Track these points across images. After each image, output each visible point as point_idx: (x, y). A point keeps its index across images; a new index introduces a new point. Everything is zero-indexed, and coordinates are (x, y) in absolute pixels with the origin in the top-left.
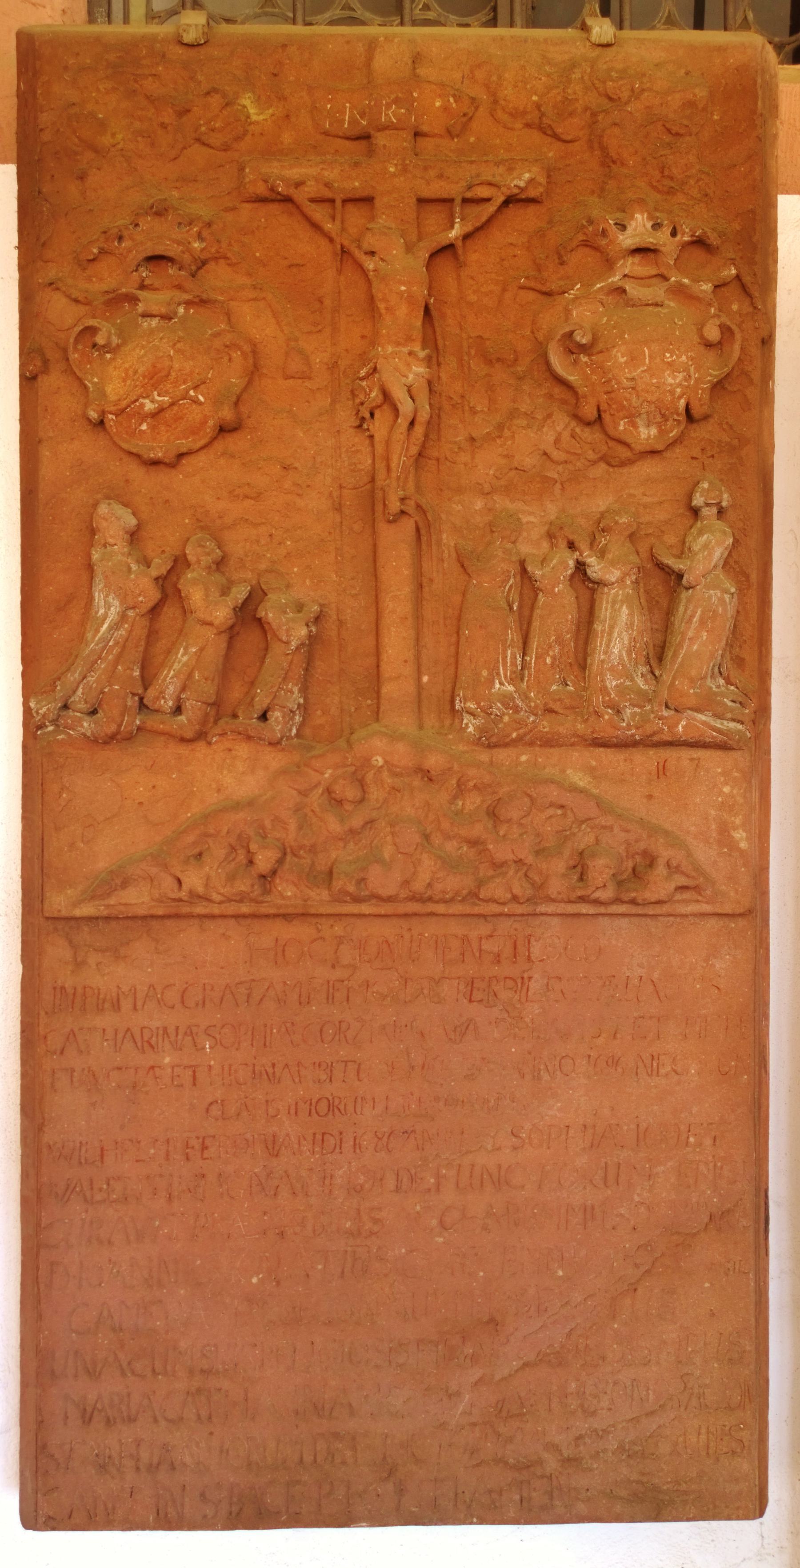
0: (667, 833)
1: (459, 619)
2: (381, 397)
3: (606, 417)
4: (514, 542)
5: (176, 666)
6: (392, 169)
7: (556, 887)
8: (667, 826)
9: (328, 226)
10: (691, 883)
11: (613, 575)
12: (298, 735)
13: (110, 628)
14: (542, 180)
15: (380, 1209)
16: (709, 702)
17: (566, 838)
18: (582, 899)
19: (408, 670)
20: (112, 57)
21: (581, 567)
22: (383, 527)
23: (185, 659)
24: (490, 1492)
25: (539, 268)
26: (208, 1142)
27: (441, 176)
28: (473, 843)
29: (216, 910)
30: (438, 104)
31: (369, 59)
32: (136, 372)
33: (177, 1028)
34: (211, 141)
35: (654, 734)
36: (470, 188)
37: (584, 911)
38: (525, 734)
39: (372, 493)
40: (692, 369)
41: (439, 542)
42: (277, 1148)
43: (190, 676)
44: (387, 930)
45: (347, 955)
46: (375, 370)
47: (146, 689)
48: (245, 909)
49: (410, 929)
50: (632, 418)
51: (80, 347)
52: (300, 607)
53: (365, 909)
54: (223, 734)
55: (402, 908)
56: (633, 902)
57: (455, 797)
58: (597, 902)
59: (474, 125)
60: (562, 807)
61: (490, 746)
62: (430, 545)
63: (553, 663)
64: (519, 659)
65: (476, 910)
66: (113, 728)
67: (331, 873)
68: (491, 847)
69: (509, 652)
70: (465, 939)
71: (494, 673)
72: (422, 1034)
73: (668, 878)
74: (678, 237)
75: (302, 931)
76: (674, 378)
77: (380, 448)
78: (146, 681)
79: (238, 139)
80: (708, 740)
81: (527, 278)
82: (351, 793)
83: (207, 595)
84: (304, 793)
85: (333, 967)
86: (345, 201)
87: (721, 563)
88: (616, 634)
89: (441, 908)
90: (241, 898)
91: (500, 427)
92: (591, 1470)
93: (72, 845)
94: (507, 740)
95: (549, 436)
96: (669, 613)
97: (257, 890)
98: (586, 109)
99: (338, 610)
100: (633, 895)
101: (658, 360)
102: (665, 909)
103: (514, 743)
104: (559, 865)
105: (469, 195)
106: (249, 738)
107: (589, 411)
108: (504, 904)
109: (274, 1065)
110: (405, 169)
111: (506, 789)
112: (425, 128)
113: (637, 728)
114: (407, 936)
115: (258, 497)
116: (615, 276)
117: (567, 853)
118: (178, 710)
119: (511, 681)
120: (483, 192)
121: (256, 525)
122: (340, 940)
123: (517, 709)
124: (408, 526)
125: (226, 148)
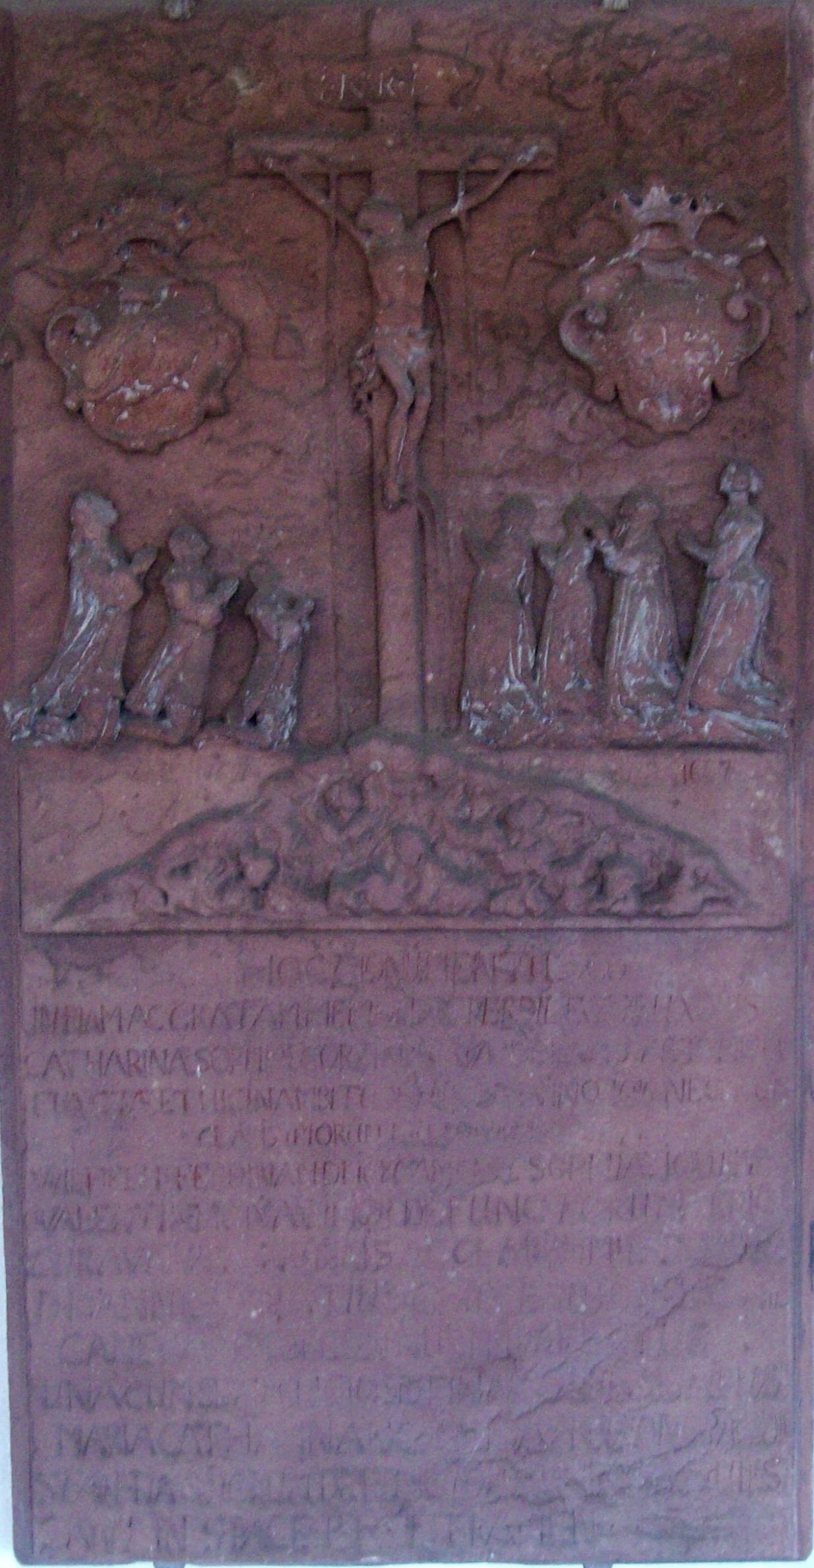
0: (693, 841)
1: (466, 613)
2: (378, 379)
3: (625, 398)
5: (159, 667)
7: (573, 901)
9: (321, 202)
10: (721, 895)
11: (633, 566)
14: (553, 150)
16: (737, 700)
18: (604, 913)
19: (412, 666)
20: (95, 34)
21: (598, 557)
23: (169, 659)
27: (443, 149)
28: (483, 853)
29: (206, 925)
30: (440, 73)
31: (366, 34)
32: (116, 360)
33: (165, 1052)
35: (678, 735)
36: (473, 160)
37: (605, 926)
38: (538, 736)
40: (716, 348)
44: (389, 947)
46: (372, 351)
47: (127, 690)
48: (235, 924)
49: (416, 946)
50: (653, 397)
51: (58, 333)
52: (292, 603)
53: (367, 924)
54: (210, 739)
56: (658, 915)
58: (619, 916)
60: (579, 814)
61: (500, 749)
63: (567, 662)
64: (531, 657)
65: (488, 925)
66: (93, 734)
67: (327, 885)
68: (501, 857)
69: (520, 649)
71: (502, 673)
74: (699, 210)
75: (297, 948)
76: (696, 357)
78: (128, 684)
80: (736, 741)
81: (539, 249)
82: (349, 800)
83: (192, 590)
85: (333, 987)
86: (339, 177)
87: (751, 551)
88: (634, 629)
89: (448, 923)
90: (231, 914)
93: (52, 859)
96: (697, 603)
97: (248, 906)
98: (597, 78)
100: (657, 907)
101: (677, 340)
103: (524, 745)
104: (577, 876)
105: (472, 168)
107: (604, 390)
108: (518, 918)
110: (402, 144)
111: (516, 796)
116: (630, 249)
117: (586, 861)
118: (162, 714)
119: (522, 680)
120: (487, 164)
121: (245, 514)
123: (528, 712)
124: (409, 515)
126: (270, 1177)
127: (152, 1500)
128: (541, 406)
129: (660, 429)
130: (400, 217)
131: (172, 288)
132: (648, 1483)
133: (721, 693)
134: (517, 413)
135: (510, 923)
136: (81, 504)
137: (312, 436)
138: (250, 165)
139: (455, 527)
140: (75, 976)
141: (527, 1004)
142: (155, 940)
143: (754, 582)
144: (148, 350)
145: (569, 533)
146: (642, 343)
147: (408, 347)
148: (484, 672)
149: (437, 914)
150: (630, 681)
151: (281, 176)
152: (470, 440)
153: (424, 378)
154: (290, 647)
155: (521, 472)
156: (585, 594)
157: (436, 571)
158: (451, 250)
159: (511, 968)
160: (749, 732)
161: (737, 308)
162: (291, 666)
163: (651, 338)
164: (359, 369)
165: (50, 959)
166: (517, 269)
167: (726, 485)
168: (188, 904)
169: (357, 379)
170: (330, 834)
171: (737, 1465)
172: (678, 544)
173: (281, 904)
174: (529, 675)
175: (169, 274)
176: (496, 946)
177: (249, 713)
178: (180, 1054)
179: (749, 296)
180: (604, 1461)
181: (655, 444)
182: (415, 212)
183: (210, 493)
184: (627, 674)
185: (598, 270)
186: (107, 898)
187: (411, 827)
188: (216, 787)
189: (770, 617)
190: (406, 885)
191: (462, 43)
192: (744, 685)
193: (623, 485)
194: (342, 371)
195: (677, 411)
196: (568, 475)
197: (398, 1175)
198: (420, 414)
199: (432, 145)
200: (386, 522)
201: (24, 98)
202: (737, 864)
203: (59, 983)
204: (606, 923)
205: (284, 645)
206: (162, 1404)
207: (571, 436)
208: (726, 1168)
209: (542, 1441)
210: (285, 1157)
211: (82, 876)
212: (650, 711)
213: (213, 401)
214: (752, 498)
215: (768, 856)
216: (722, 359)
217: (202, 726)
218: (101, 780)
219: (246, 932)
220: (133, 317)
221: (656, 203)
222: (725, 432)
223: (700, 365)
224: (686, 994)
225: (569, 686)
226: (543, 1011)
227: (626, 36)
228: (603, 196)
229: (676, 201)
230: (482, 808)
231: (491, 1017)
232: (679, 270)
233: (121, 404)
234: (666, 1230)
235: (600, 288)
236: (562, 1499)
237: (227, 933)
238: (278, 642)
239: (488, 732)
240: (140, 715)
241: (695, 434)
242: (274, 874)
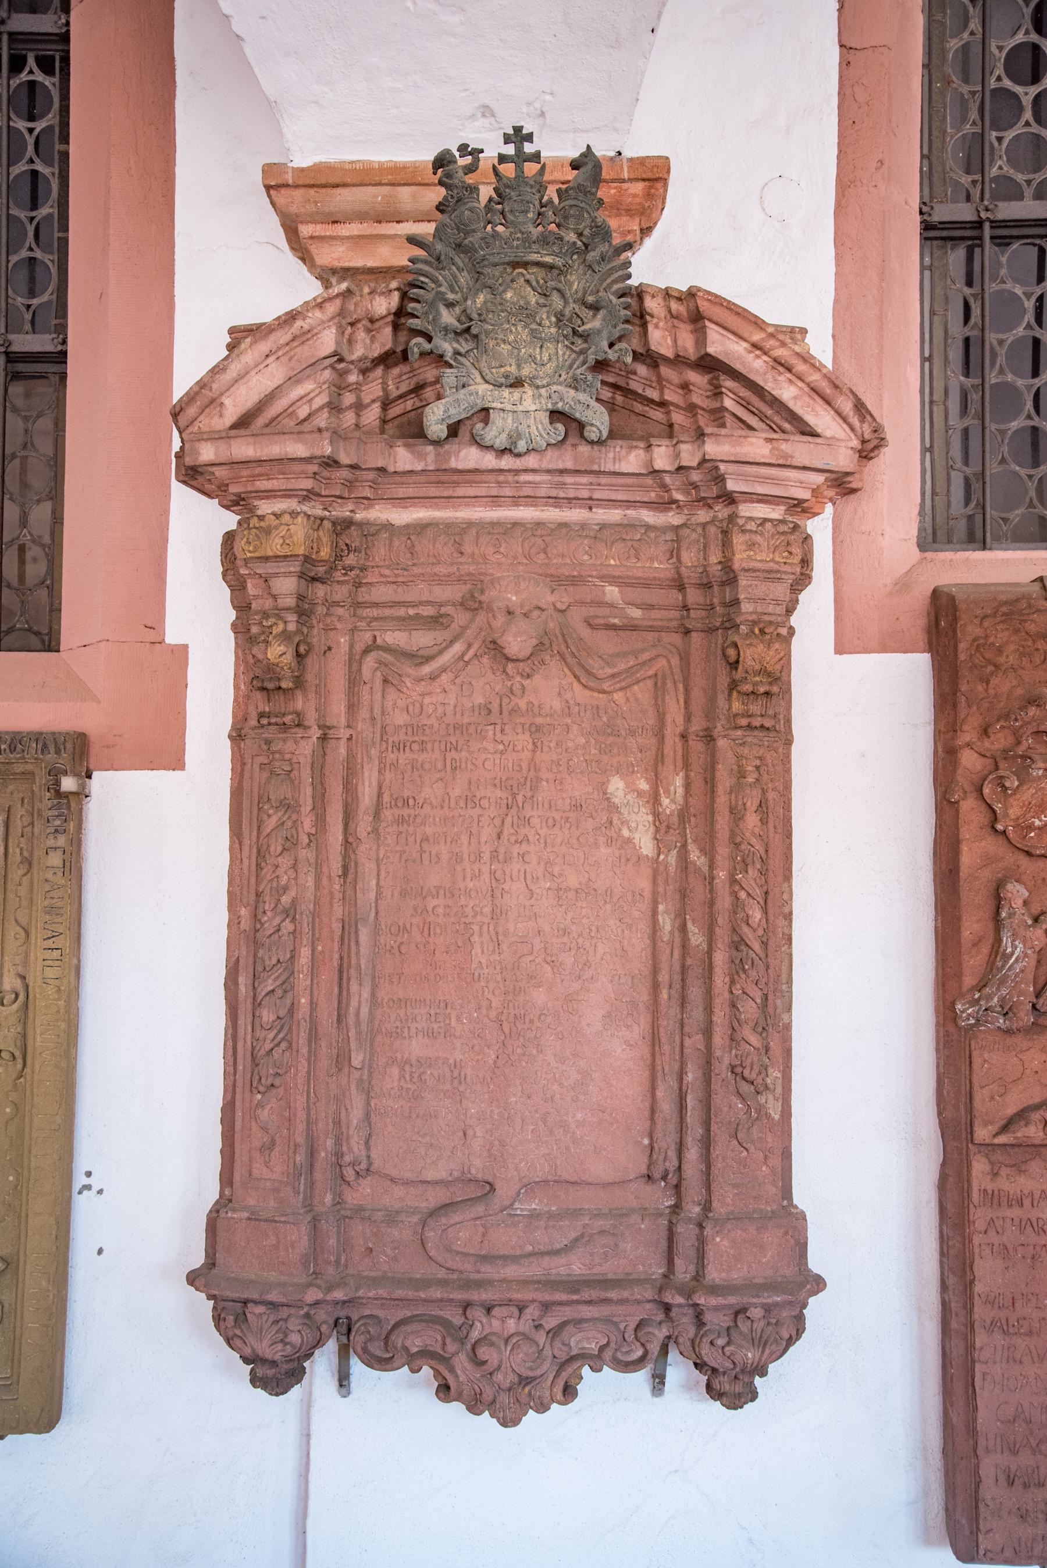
13: (1017, 960)
20: (1004, 609)
93: (992, 1098)
140: (1004, 1171)
165: (989, 1160)
201: (962, 646)
203: (995, 1175)
211: (1011, 1110)
218: (1022, 1052)
220: (1039, 778)
233: (1031, 827)
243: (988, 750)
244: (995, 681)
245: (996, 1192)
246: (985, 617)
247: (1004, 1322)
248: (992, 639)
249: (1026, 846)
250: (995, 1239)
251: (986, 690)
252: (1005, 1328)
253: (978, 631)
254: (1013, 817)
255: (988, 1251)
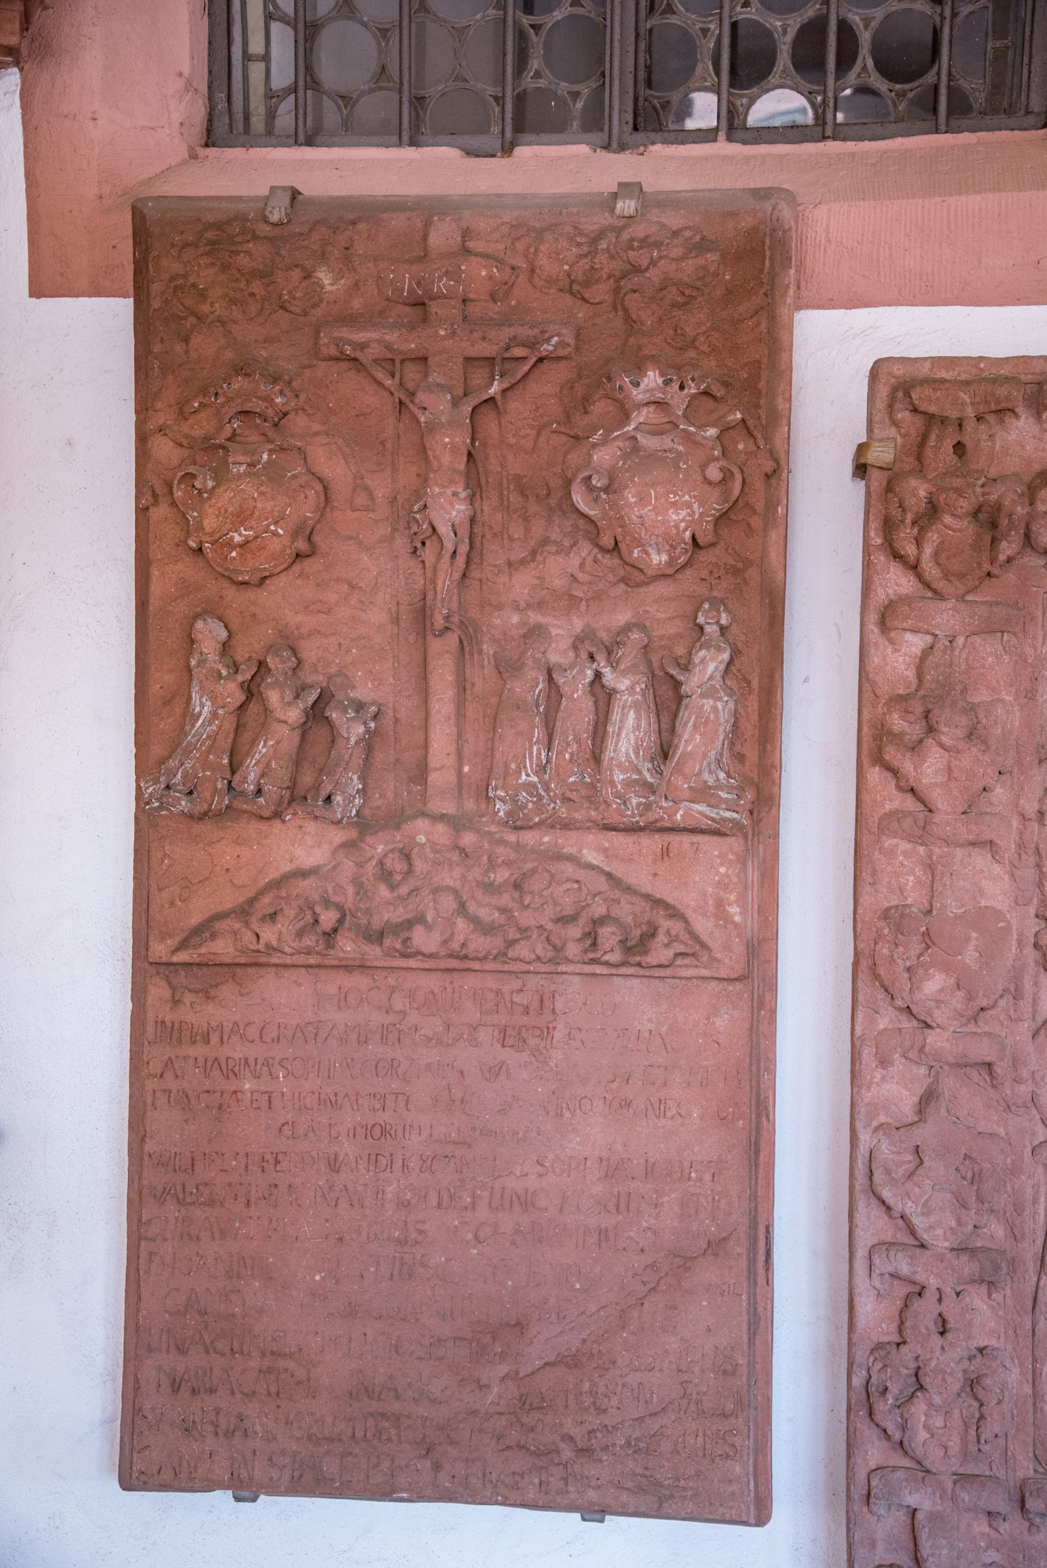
0: (667, 906)
1: (495, 718)
2: (430, 530)
3: (622, 546)
4: (544, 653)
5: (257, 756)
6: (442, 333)
7: (573, 950)
8: (669, 900)
9: (389, 382)
10: (689, 951)
11: (623, 684)
12: (358, 814)
15: (424, 1222)
16: (703, 793)
17: (583, 908)
18: (594, 961)
19: (451, 761)
20: (210, 235)
21: (598, 675)
22: (430, 638)
23: (264, 751)
24: (514, 1473)
25: (568, 416)
26: (280, 1157)
27: (484, 339)
28: (503, 910)
29: (289, 961)
30: (483, 273)
31: (425, 237)
33: (256, 1059)
34: (292, 309)
35: (656, 821)
36: (508, 348)
38: (546, 819)
39: (423, 609)
40: (696, 506)
41: (480, 652)
42: (338, 1165)
43: (268, 765)
44: (431, 982)
45: (399, 1002)
46: (425, 506)
47: (233, 773)
48: (312, 960)
49: (452, 982)
51: (183, 486)
52: (360, 707)
53: (412, 963)
54: (295, 814)
55: (444, 964)
56: (639, 965)
57: (487, 872)
58: (607, 964)
59: (516, 291)
60: (577, 882)
61: (517, 828)
62: (471, 654)
63: (571, 760)
65: (506, 968)
66: (205, 807)
68: (516, 914)
69: (535, 748)
70: (498, 992)
71: (521, 766)
72: (461, 1072)
73: (667, 946)
74: (686, 391)
75: (360, 981)
76: (678, 514)
77: (429, 574)
79: (314, 306)
80: (703, 827)
82: (398, 866)
83: (283, 698)
84: (360, 865)
85: (387, 1012)
86: (403, 361)
88: (623, 735)
89: (476, 965)
91: (534, 553)
92: (601, 1461)
93: (172, 903)
94: (531, 824)
95: (576, 561)
97: (321, 946)
98: (609, 277)
99: (395, 710)
100: (638, 959)
102: (668, 972)
103: (538, 825)
104: (575, 931)
105: (507, 355)
106: (316, 817)
107: (607, 541)
108: (529, 963)
109: (336, 1095)
110: (454, 333)
111: (529, 866)
112: (472, 296)
113: (641, 816)
114: (449, 989)
115: (329, 612)
116: (629, 425)
117: (582, 921)
118: (259, 792)
119: (536, 774)
120: (518, 352)
121: (326, 636)
122: (393, 990)
123: (540, 797)
124: (452, 640)
125: (305, 313)
126: (334, 1165)
127: (229, 1434)
128: (558, 553)
129: (650, 573)
130: (449, 397)
131: (271, 452)
132: (628, 1443)
133: (690, 788)
134: (539, 558)
135: (526, 967)
136: (199, 625)
137: (379, 574)
138: (333, 351)
139: (488, 649)
140: (188, 997)
141: (538, 1032)
142: (250, 970)
143: (720, 699)
144: (251, 503)
145: (577, 656)
146: (635, 503)
147: (452, 504)
148: (506, 766)
149: (466, 957)
150: (619, 777)
151: (355, 360)
152: (503, 579)
153: (463, 532)
154: (356, 743)
155: (540, 606)
156: (588, 704)
157: (473, 684)
158: (490, 424)
159: (525, 1003)
160: (713, 820)
161: (714, 473)
162: (358, 760)
163: (642, 500)
164: (416, 520)
166: (542, 439)
167: (701, 620)
168: (275, 943)
169: (415, 528)
170: (384, 891)
171: (701, 1434)
172: (662, 668)
173: (347, 946)
174: (541, 770)
175: (270, 441)
176: (516, 984)
177: (324, 794)
178: (267, 1063)
179: (723, 463)
180: (594, 1421)
181: (648, 584)
182: (460, 392)
183: (299, 618)
184: (616, 771)
185: (604, 442)
186: (213, 937)
187: (448, 888)
188: (299, 852)
189: (735, 725)
190: (442, 933)
191: (501, 246)
192: (711, 781)
193: (622, 618)
194: (402, 525)
195: (664, 558)
196: (578, 609)
197: (434, 1168)
198: (461, 560)
199: (476, 335)
200: (435, 645)
202: (703, 926)
203: (176, 1002)
204: (598, 969)
205: (352, 742)
206: (242, 1353)
207: (580, 576)
208: (693, 1175)
209: (543, 1399)
210: (348, 1149)
211: (196, 920)
212: (634, 801)
213: (302, 545)
214: (723, 629)
215: (728, 919)
216: (701, 514)
217: (289, 803)
218: (211, 843)
219: (319, 966)
220: (240, 476)
221: (652, 385)
222: (704, 574)
223: (683, 520)
224: (664, 1029)
225: (572, 779)
226: (549, 1039)
227: (632, 240)
228: (609, 379)
229: (667, 382)
230: (501, 876)
231: (509, 1041)
232: (666, 442)
233: (231, 545)
234: (644, 1224)
235: (604, 457)
236: (557, 1451)
237: (308, 967)
238: (348, 739)
239: (509, 814)
240: (242, 793)
241: (679, 576)
242: (341, 921)
243: (186, 436)
244: (196, 340)
245: (177, 1025)
246: (186, 245)
247: (179, 1188)
248: (192, 279)
249: (228, 569)
250: (172, 1084)
251: (187, 352)
252: (181, 1196)
253: (177, 267)
254: (208, 530)
255: (162, 1099)
